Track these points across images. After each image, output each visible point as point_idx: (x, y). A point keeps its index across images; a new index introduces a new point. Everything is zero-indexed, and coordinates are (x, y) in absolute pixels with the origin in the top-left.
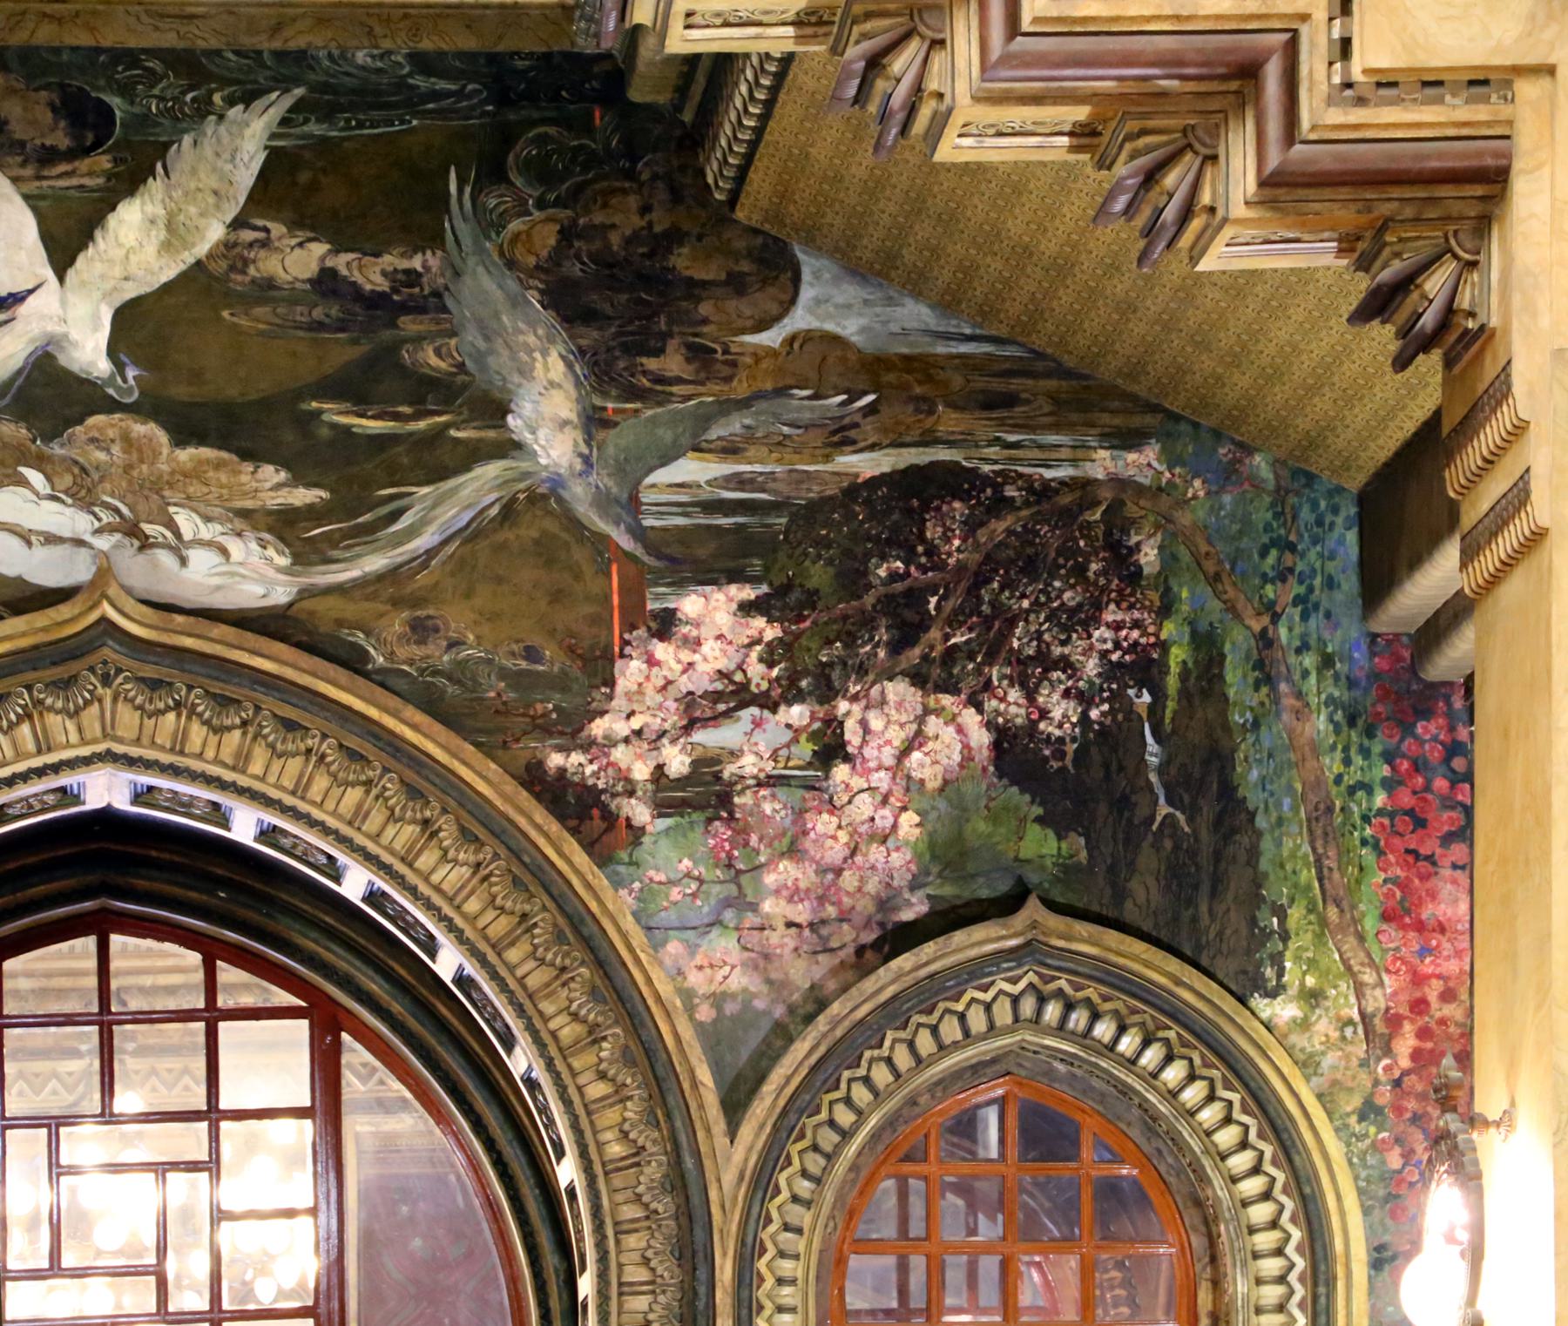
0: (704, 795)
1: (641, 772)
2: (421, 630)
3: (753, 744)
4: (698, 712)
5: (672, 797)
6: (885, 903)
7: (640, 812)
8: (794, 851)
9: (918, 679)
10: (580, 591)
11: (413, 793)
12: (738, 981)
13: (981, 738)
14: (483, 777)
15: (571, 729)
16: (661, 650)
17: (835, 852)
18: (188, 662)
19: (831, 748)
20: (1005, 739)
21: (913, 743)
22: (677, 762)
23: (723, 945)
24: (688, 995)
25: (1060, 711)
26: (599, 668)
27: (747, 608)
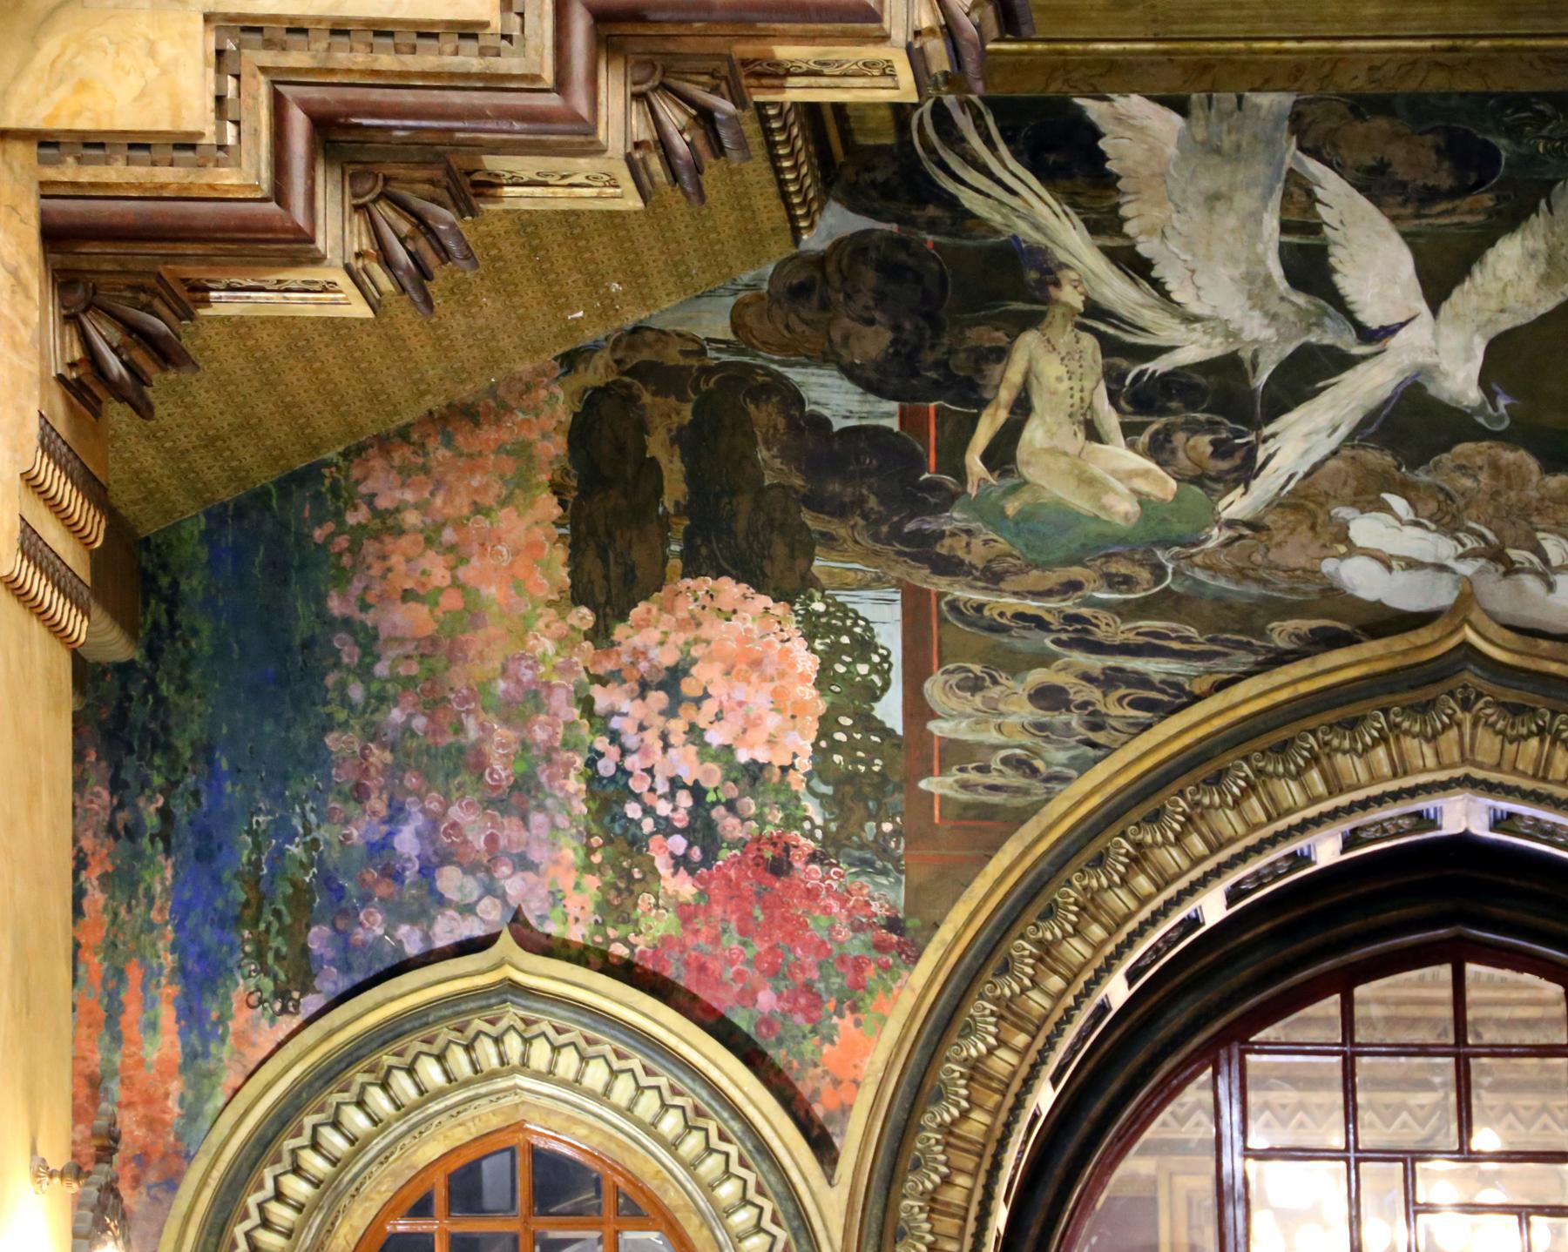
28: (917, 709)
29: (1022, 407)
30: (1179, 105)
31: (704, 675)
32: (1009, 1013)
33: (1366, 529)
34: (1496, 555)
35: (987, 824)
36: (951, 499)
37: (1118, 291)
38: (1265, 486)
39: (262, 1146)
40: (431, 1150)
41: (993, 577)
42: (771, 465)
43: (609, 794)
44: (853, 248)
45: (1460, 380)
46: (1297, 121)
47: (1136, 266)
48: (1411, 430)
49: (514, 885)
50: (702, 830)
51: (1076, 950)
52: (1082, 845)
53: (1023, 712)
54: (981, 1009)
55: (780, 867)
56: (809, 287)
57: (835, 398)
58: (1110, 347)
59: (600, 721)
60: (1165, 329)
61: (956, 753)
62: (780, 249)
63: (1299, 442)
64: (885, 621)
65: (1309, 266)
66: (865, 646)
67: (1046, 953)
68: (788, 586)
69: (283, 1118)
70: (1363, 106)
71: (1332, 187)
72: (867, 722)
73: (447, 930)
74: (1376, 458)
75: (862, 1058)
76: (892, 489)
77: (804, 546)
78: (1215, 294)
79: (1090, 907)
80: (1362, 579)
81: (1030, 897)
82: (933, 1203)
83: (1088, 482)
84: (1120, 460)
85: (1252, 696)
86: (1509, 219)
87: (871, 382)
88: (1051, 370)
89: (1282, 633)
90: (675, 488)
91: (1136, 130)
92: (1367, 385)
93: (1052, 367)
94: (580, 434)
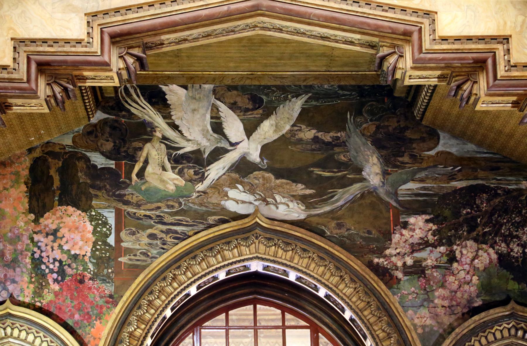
0: (417, 270)
1: (400, 264)
2: (340, 226)
3: (430, 257)
4: (414, 248)
5: (407, 270)
6: (470, 301)
7: (399, 275)
8: (443, 286)
9: (476, 240)
10: (382, 216)
11: (338, 268)
12: (429, 322)
13: (494, 256)
14: (356, 265)
15: (380, 252)
16: (404, 232)
17: (455, 286)
18: (277, 234)
19: (452, 258)
20: (501, 257)
21: (475, 259)
22: (409, 261)
23: (424, 312)
24: (415, 326)
25: (517, 250)
26: (387, 236)
27: (427, 221)
28: (118, 240)
30: (185, 87)
31: (63, 231)
32: (140, 319)
33: (232, 193)
34: (264, 200)
35: (136, 270)
36: (128, 186)
37: (170, 133)
41: (138, 206)
42: (82, 177)
43: (37, 262)
44: (104, 122)
45: (255, 156)
46: (214, 91)
47: (175, 127)
48: (243, 168)
49: (11, 287)
50: (61, 272)
51: (158, 302)
53: (146, 240)
54: (133, 318)
55: (82, 282)
56: (92, 132)
58: (168, 147)
60: (182, 143)
61: (128, 251)
62: (85, 122)
63: (216, 171)
64: (111, 217)
65: (218, 128)
67: (150, 303)
68: (86, 208)
70: (230, 88)
71: (223, 108)
72: (105, 243)
74: (235, 175)
76: (113, 183)
77: (90, 198)
78: (195, 135)
79: (162, 291)
80: (231, 206)
81: (147, 289)
83: (163, 181)
85: (204, 236)
86: (267, 115)
87: (108, 156)
88: (154, 153)
89: (211, 220)
90: (57, 183)
91: (175, 93)
93: (154, 153)
94: (32, 169)
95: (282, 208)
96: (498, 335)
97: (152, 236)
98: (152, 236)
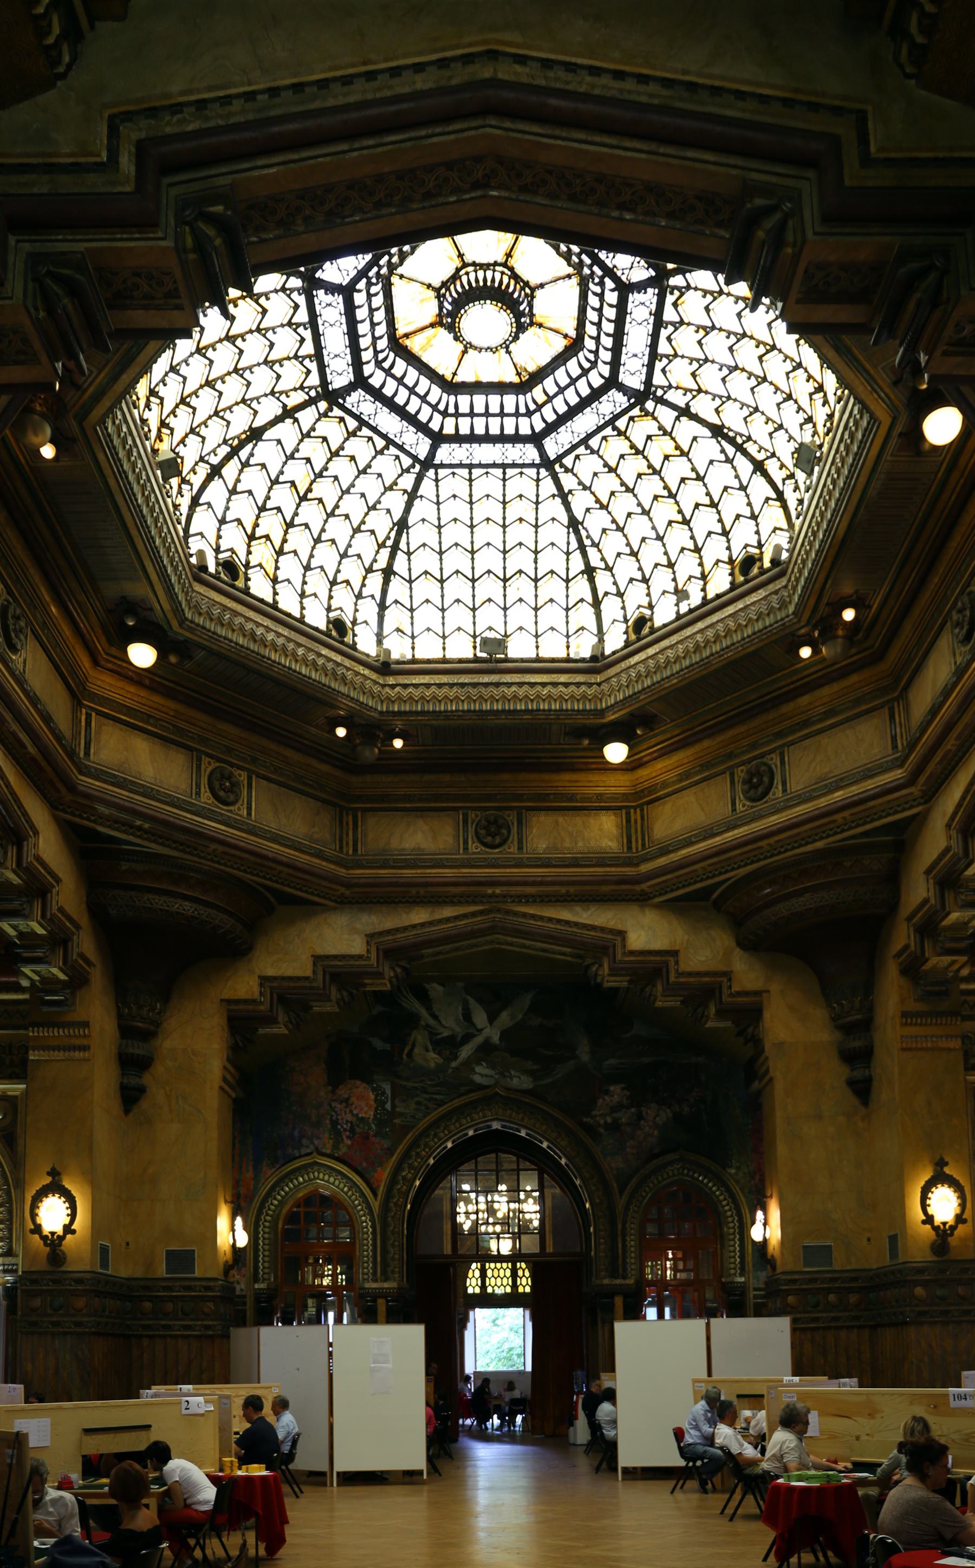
0: (614, 1127)
1: (602, 1122)
4: (615, 1109)
7: (602, 1130)
13: (670, 1115)
16: (606, 1097)
19: (640, 1117)
21: (657, 1115)
22: (609, 1120)
28: (393, 1106)
29: (414, 1046)
30: (443, 985)
31: (353, 1099)
33: (478, 1069)
35: (406, 1129)
37: (432, 1022)
38: (460, 1060)
39: (268, 1195)
40: (301, 1195)
43: (334, 1123)
45: (496, 1039)
47: (435, 1017)
48: (486, 1049)
49: (316, 1142)
50: (352, 1130)
52: (425, 1133)
55: (367, 1138)
57: (378, 1044)
59: (333, 1109)
61: (401, 1115)
63: (466, 1052)
64: (387, 1088)
65: (467, 1017)
66: (384, 1093)
68: (369, 1081)
69: (273, 1189)
71: (472, 1002)
73: (303, 1151)
75: (383, 1175)
78: (450, 1024)
80: (477, 1079)
81: (414, 1144)
82: (396, 1204)
84: (432, 1055)
85: (456, 1103)
88: (419, 1038)
91: (436, 990)
92: (479, 1040)
93: (420, 1037)
95: (515, 1081)
96: (670, 1173)
97: (418, 1103)
98: (418, 1103)
